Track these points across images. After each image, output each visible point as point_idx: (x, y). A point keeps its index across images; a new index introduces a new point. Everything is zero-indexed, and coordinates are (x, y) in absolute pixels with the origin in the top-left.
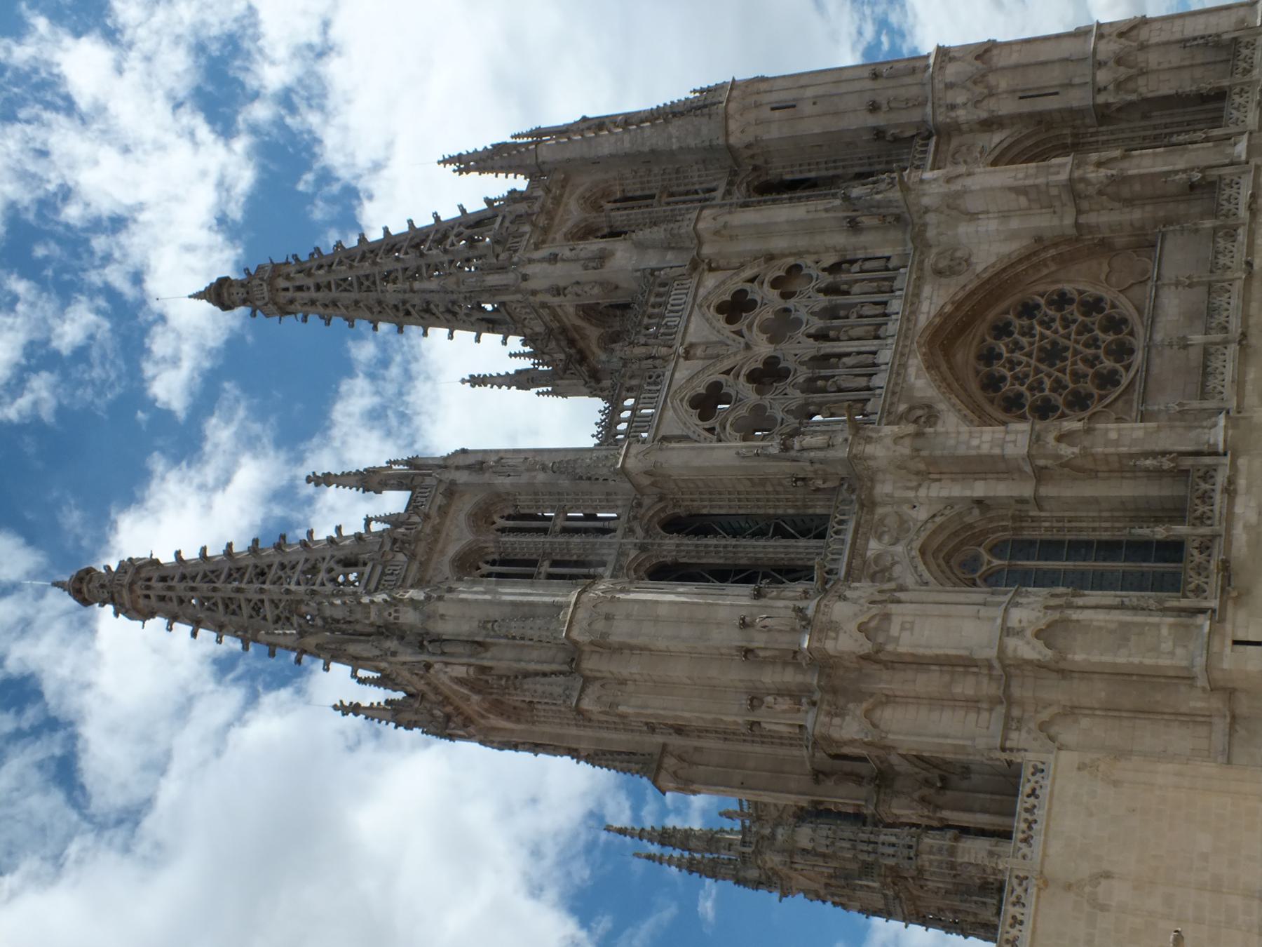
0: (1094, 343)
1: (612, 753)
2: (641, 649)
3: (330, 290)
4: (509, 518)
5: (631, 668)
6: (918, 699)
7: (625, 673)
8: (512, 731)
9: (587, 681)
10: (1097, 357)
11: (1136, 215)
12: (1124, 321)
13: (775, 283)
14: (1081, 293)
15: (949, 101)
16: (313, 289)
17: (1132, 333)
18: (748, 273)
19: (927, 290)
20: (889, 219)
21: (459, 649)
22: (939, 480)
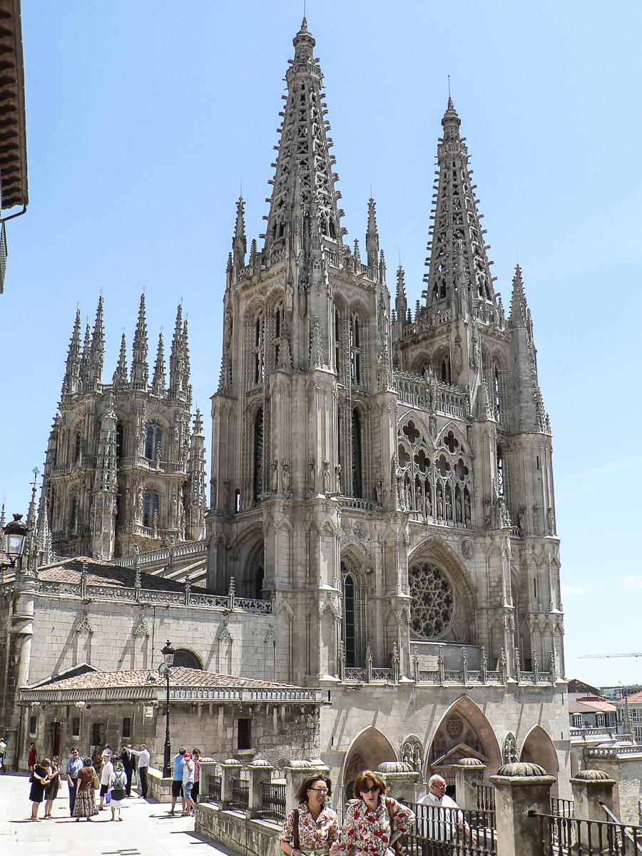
0: (431, 618)
1: (231, 370)
2: (309, 407)
3: (454, 194)
4: (356, 322)
5: (299, 401)
6: (291, 548)
7: (297, 398)
8: (239, 311)
9: (289, 376)
10: (426, 620)
11: (485, 636)
12: (440, 631)
13: (461, 461)
14: (452, 610)
15: (536, 546)
16: (455, 183)
17: (435, 635)
18: (466, 447)
19: (456, 538)
20: (489, 519)
21: (302, 305)
22: (382, 553)
